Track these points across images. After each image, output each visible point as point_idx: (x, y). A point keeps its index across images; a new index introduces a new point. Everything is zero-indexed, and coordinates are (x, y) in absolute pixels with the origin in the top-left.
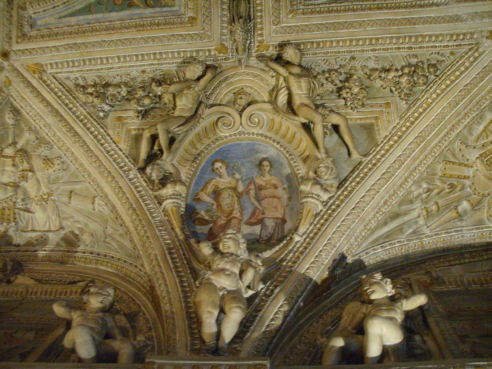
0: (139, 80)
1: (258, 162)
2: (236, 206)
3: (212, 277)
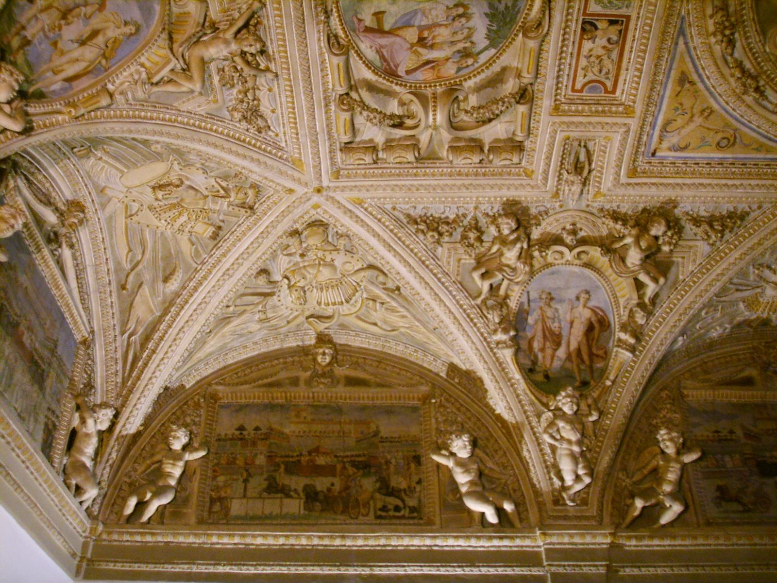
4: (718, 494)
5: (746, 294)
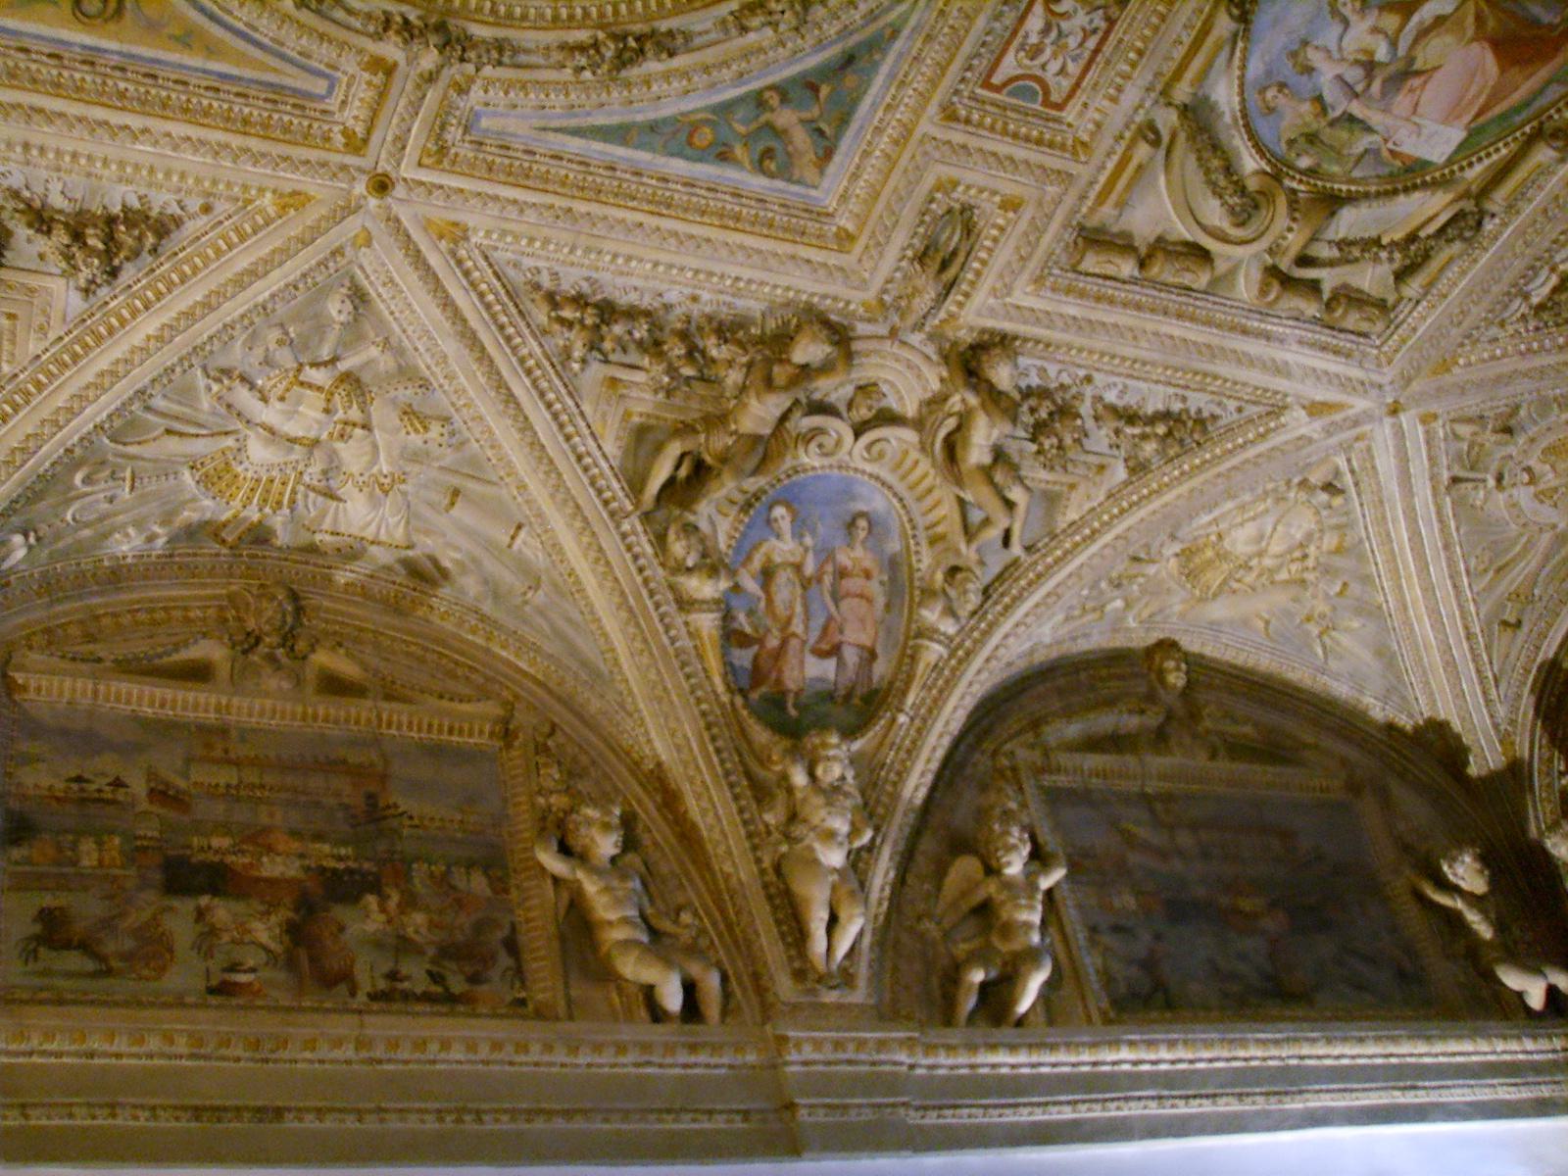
0: (678, 311)
1: (848, 519)
2: (799, 609)
3: (817, 846)
4: (37, 929)
5: (199, 447)
